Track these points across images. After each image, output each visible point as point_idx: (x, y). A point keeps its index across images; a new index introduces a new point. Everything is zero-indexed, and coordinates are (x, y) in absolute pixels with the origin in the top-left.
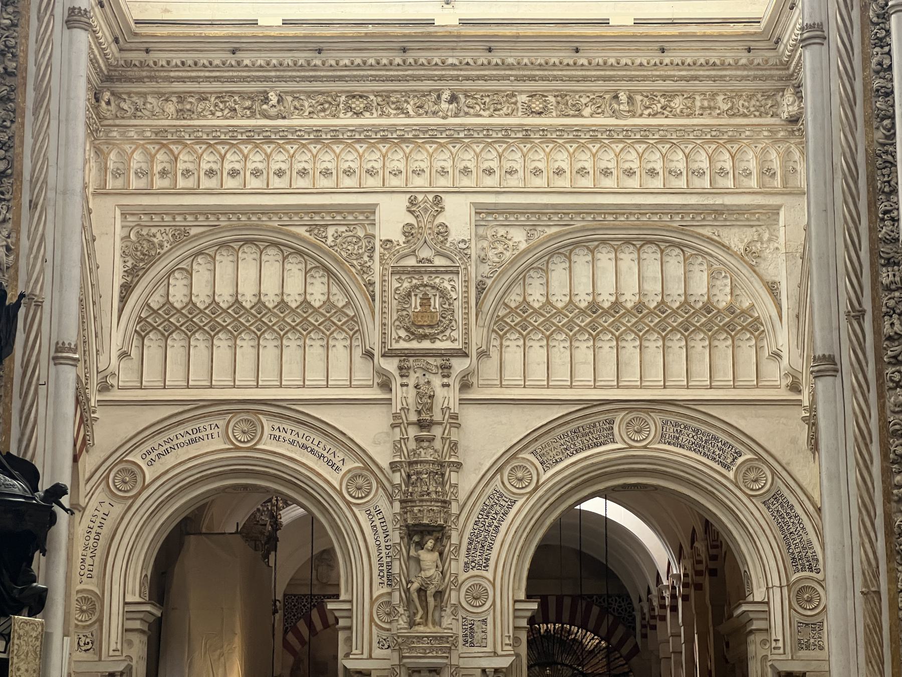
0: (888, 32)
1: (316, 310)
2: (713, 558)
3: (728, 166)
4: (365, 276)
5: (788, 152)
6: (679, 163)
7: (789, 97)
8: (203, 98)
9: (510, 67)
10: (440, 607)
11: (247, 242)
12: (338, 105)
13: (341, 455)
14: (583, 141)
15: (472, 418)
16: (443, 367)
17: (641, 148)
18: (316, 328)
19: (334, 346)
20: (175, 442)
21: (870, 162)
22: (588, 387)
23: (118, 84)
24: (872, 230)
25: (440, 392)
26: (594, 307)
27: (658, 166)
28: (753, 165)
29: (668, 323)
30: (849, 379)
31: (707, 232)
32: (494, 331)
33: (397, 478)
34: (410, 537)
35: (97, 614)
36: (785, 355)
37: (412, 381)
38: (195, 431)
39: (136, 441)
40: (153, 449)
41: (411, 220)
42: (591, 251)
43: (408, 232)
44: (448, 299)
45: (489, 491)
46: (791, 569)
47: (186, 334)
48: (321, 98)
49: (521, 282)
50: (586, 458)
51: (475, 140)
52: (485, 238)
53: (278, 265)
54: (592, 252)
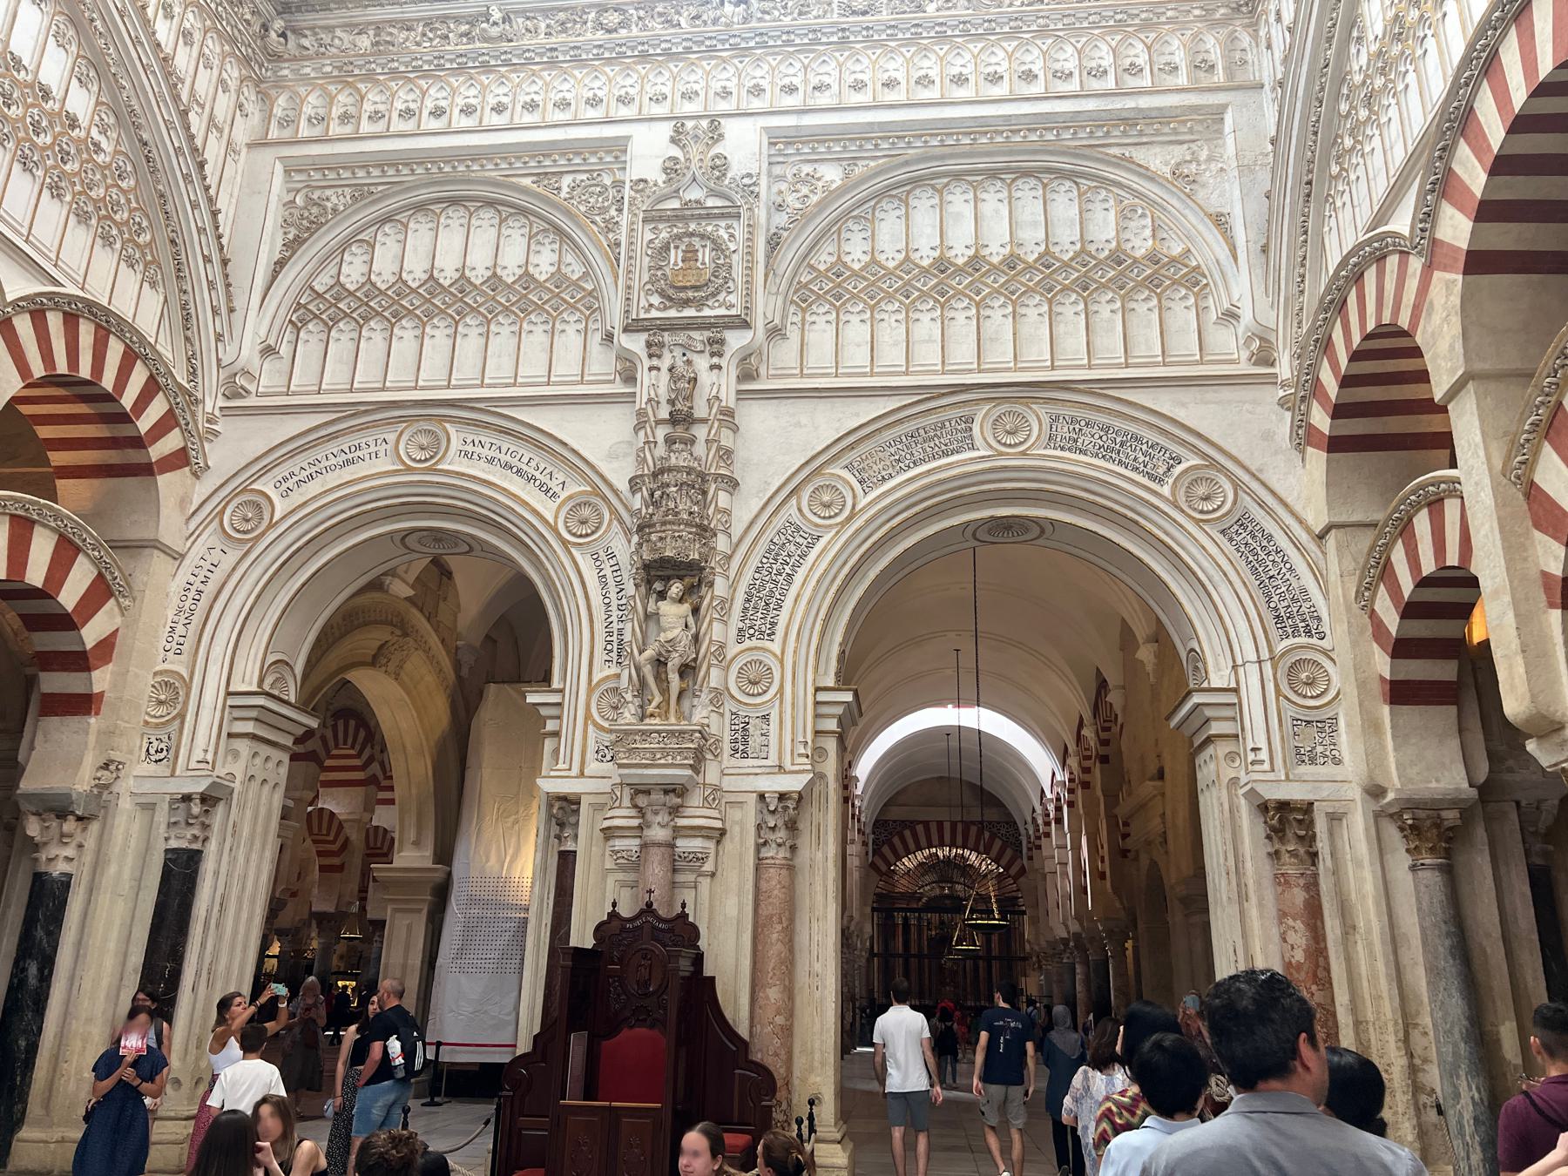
1: (540, 285)
2: (1104, 743)
4: (611, 235)
5: (1233, 38)
6: (1068, 59)
12: (586, 23)
13: (560, 477)
14: (925, 42)
15: (758, 420)
16: (711, 342)
18: (539, 308)
19: (563, 331)
20: (325, 463)
22: (935, 372)
23: (298, 16)
25: (706, 378)
28: (1180, 58)
29: (1057, 281)
32: (792, 302)
33: (637, 502)
34: (649, 583)
35: (179, 707)
37: (665, 363)
38: (353, 449)
39: (265, 463)
40: (292, 474)
41: (676, 152)
42: (937, 191)
43: (672, 169)
44: (723, 251)
45: (779, 522)
46: (1274, 633)
47: (357, 322)
48: (562, 16)
49: (835, 236)
50: (929, 472)
51: (771, 50)
52: (782, 178)
53: (493, 232)
54: (940, 192)
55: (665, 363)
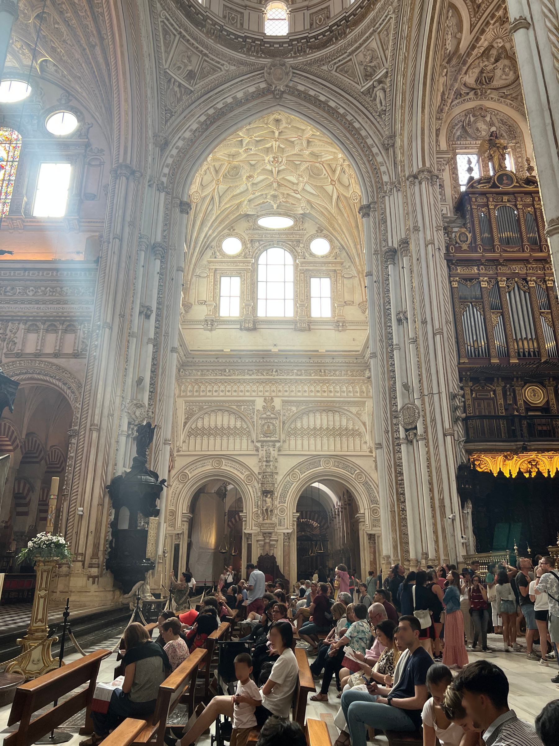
0: (393, 355)
1: (238, 429)
2: (349, 500)
3: (351, 390)
5: (368, 386)
7: (367, 372)
8: (208, 371)
9: (292, 363)
10: (272, 515)
11: (219, 410)
13: (244, 470)
15: (282, 460)
17: (327, 385)
21: (390, 389)
24: (390, 409)
25: (272, 452)
26: (315, 428)
27: (332, 390)
28: (358, 390)
30: (385, 450)
31: (346, 408)
33: (260, 477)
34: (263, 494)
36: (368, 442)
37: (264, 449)
39: (186, 466)
43: (264, 408)
45: (286, 480)
46: (371, 504)
53: (228, 417)
55: (264, 449)
